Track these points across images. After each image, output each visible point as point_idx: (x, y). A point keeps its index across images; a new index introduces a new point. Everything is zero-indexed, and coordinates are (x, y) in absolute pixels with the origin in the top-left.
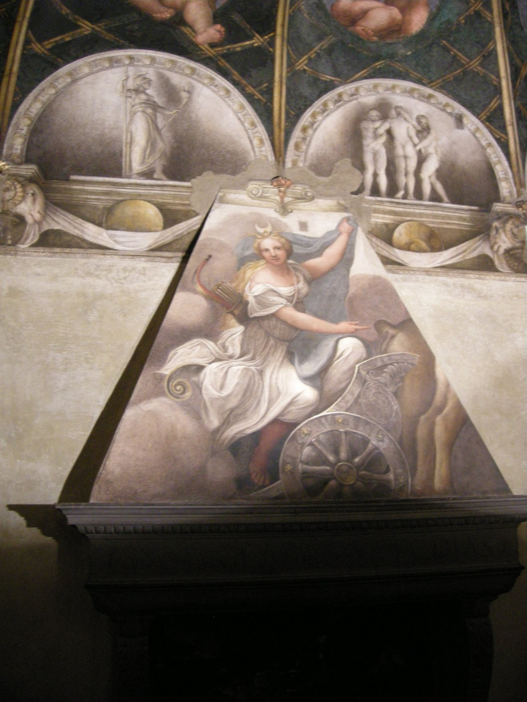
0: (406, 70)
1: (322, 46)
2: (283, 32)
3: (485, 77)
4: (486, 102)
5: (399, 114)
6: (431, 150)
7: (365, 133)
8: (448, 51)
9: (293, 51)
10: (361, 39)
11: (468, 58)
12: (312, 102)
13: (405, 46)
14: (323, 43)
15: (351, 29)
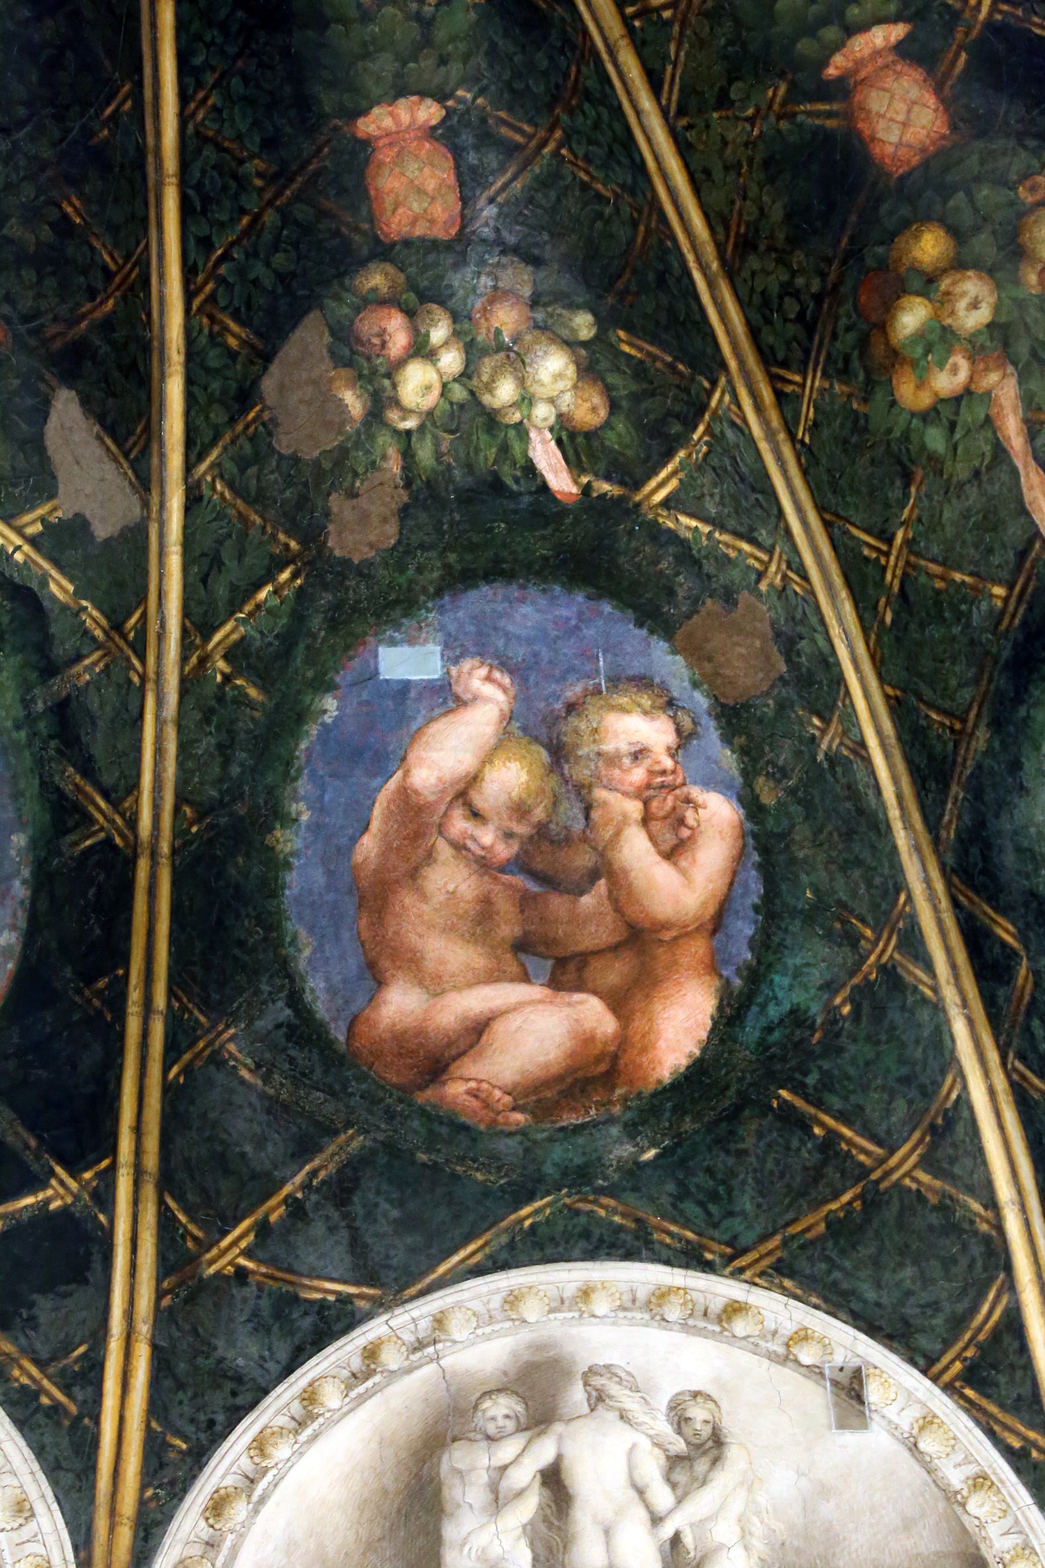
0: (638, 1220)
1: (314, 1173)
2: (138, 1151)
3: (946, 1207)
4: (961, 1307)
5: (598, 1399)
6: (724, 1532)
7: (453, 1492)
8: (804, 1125)
9: (187, 1211)
10: (465, 1128)
11: (880, 1143)
12: (266, 1392)
13: (632, 1130)
14: (317, 1162)
15: (425, 1097)
